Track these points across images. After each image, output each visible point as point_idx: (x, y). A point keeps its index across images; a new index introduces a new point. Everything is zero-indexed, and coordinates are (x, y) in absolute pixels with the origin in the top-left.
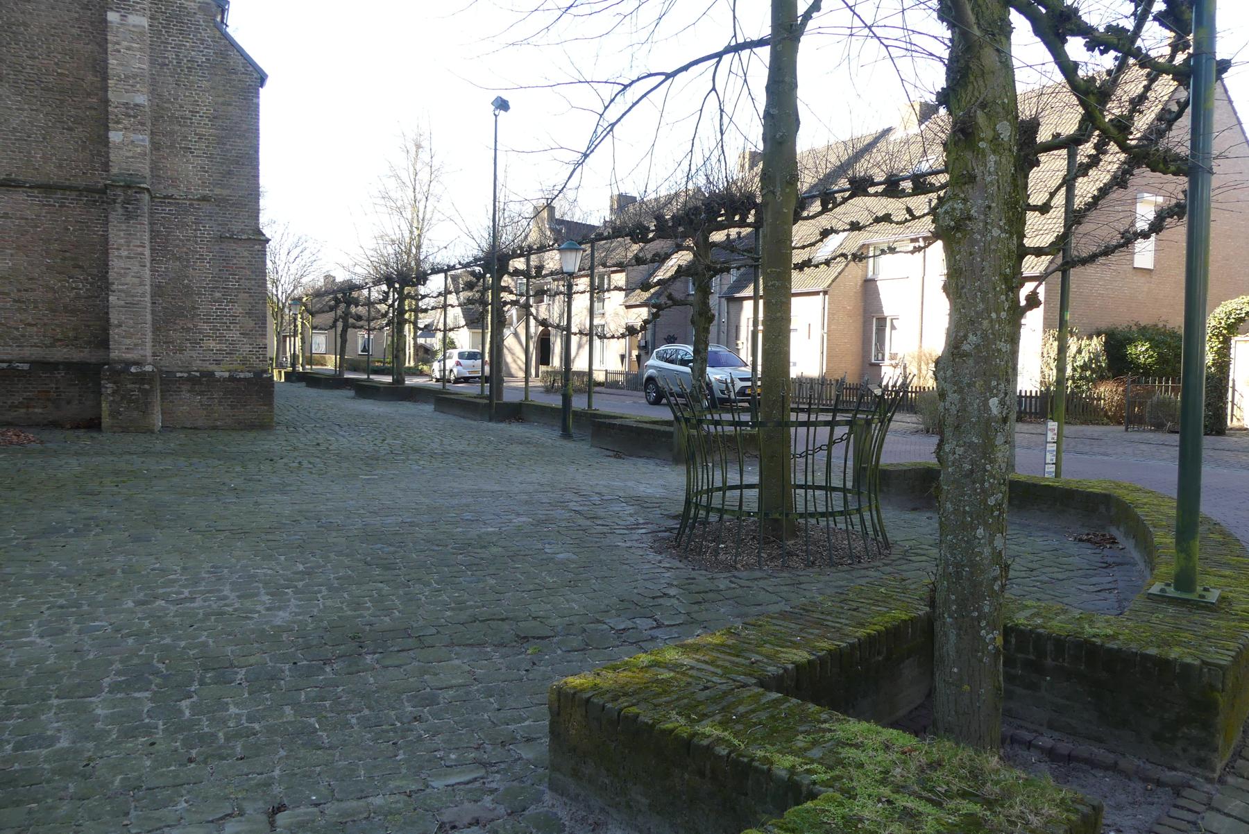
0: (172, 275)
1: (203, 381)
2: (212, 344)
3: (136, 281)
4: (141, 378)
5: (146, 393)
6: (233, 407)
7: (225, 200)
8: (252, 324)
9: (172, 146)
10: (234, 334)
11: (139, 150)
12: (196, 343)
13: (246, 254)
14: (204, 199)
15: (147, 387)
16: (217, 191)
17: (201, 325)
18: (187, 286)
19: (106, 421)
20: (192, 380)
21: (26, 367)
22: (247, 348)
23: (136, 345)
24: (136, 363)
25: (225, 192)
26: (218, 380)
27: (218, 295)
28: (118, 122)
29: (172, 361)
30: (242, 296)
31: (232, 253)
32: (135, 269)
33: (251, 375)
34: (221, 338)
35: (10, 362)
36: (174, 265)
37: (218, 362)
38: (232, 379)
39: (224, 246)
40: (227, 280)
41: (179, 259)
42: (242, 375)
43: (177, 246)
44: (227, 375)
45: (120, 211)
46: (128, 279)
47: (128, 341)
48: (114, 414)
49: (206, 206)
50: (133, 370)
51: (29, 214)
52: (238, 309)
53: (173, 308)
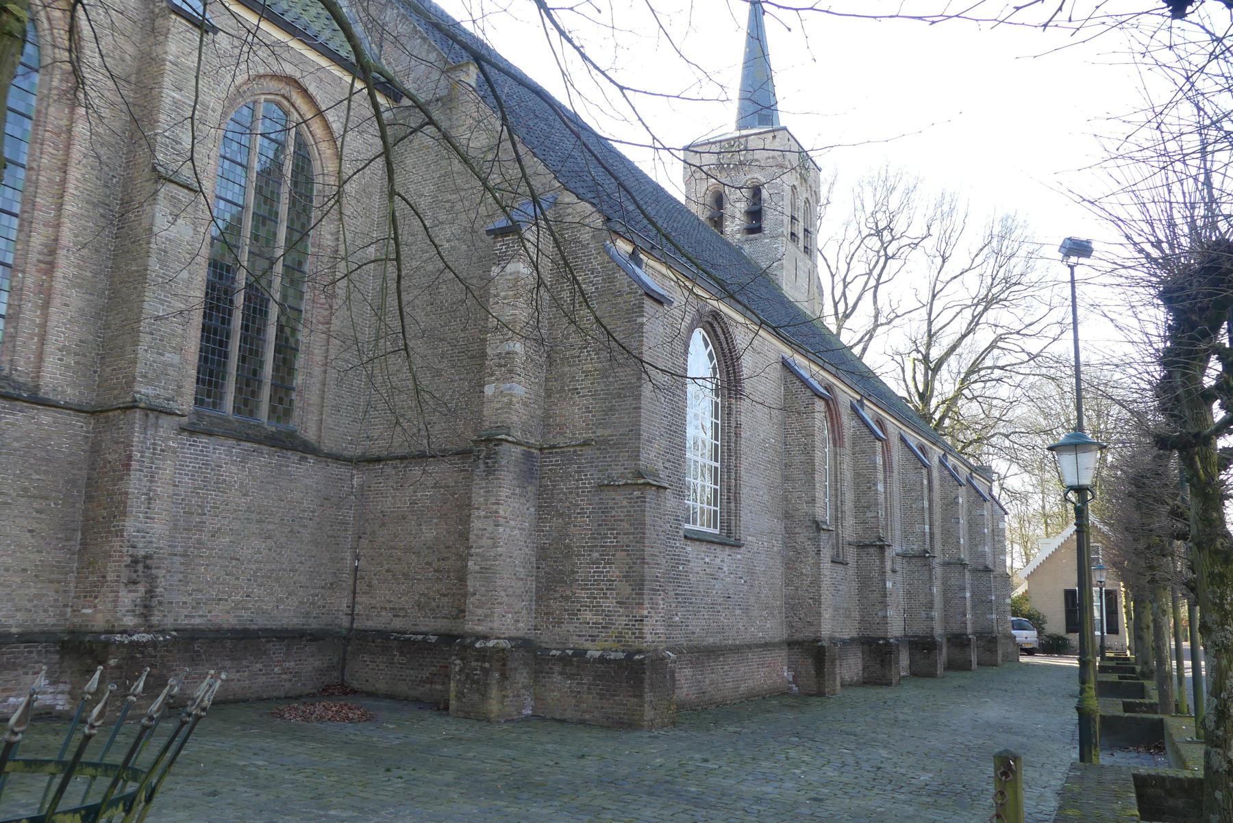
0: (555, 534)
1: (574, 661)
2: (588, 616)
3: (490, 542)
4: (483, 655)
5: (486, 672)
6: (602, 696)
7: (606, 442)
8: (629, 590)
9: (562, 390)
10: (609, 604)
11: (506, 400)
12: (574, 614)
13: (625, 503)
14: (586, 443)
15: (487, 665)
16: (599, 432)
18: (568, 547)
19: (453, 703)
20: (564, 660)
21: (433, 639)
22: (623, 621)
23: (486, 616)
24: (486, 638)
25: (607, 432)
26: (588, 662)
27: (596, 555)
28: (492, 375)
29: (548, 637)
30: (621, 555)
31: (611, 504)
32: (490, 529)
33: (621, 655)
34: (597, 609)
35: (426, 634)
36: (557, 522)
37: (593, 638)
38: (602, 660)
39: (603, 496)
40: (605, 536)
41: (561, 515)
42: (613, 656)
43: (561, 500)
44: (597, 654)
45: (482, 467)
46: (485, 542)
47: (480, 611)
48: (460, 695)
49: (588, 451)
50: (477, 645)
51: (451, 482)
52: (615, 572)
53: (552, 575)
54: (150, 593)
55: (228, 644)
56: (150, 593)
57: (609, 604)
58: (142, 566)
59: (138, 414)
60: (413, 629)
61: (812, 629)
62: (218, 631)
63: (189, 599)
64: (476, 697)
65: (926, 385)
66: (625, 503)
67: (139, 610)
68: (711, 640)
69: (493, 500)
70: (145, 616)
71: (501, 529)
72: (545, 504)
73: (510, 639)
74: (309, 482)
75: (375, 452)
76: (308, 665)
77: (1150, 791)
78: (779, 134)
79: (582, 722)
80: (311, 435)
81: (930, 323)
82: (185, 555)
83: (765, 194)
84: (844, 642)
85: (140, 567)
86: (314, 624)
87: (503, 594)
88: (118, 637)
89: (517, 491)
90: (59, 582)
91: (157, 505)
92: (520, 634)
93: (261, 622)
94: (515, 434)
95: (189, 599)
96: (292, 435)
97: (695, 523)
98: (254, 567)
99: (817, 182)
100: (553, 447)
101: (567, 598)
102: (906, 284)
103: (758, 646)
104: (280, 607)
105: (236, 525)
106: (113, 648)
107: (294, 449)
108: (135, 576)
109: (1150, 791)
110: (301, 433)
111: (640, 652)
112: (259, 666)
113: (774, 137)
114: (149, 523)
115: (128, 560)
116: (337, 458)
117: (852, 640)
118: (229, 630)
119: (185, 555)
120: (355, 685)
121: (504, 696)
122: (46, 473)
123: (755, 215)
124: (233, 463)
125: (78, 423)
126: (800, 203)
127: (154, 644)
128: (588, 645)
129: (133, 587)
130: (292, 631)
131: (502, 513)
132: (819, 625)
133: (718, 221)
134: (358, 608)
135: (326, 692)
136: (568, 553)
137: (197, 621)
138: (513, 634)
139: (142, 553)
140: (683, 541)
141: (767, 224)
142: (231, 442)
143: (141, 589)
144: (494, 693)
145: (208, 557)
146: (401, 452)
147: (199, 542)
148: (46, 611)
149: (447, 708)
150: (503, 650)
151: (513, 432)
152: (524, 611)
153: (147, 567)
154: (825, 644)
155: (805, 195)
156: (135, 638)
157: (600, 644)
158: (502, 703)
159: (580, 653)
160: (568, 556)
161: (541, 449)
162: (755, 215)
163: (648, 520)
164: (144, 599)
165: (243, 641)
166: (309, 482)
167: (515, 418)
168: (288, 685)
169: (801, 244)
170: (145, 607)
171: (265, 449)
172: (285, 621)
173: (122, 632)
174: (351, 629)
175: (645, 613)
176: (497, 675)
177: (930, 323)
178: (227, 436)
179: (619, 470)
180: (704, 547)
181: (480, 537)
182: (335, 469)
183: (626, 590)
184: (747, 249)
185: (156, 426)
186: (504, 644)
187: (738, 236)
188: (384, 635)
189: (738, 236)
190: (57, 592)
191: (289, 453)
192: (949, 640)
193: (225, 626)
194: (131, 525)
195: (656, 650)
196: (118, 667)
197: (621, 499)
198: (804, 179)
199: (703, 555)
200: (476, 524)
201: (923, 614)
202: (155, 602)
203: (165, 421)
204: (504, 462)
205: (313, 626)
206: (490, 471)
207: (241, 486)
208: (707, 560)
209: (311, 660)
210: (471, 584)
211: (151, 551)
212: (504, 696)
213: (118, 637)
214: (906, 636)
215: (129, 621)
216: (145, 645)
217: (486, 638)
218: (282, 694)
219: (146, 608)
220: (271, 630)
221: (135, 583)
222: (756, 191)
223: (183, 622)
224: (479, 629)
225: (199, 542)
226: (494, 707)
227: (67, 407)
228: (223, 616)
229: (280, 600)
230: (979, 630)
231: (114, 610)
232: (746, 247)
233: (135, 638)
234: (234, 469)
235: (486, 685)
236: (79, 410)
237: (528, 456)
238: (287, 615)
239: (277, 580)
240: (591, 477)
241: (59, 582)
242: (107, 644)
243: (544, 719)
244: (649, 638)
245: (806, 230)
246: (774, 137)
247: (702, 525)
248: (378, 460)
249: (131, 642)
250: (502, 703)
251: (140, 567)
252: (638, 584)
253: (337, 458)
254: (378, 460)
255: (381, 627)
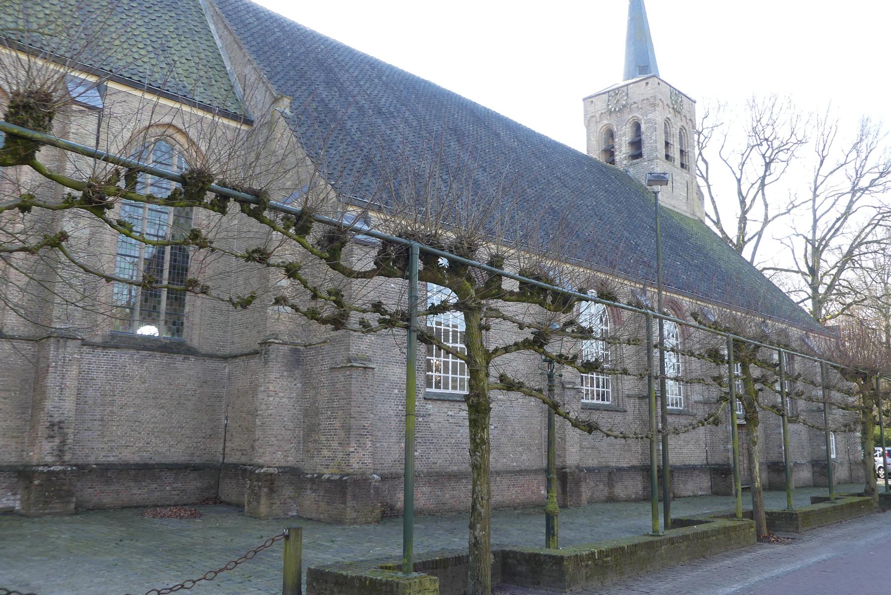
1: (317, 481)
4: (259, 477)
5: (260, 488)
6: (328, 504)
12: (319, 451)
14: (325, 342)
17: (323, 438)
18: (317, 408)
20: (312, 480)
33: (338, 477)
34: (329, 448)
36: (313, 392)
38: (329, 480)
46: (264, 407)
47: (261, 450)
48: (249, 502)
49: (327, 347)
52: (337, 424)
53: (309, 427)
54: (63, 442)
55: (132, 472)
56: (63, 442)
57: (335, 444)
58: (56, 428)
59: (52, 340)
60: (250, 462)
61: (561, 460)
62: (126, 465)
63: (106, 446)
64: (255, 503)
65: (814, 262)
66: (342, 379)
67: (55, 453)
68: (455, 468)
69: (267, 380)
70: (60, 456)
71: (271, 399)
72: (308, 382)
73: (278, 468)
74: (191, 372)
75: (235, 352)
76: (193, 485)
77: (510, 561)
78: (650, 81)
79: (319, 521)
80: (195, 343)
81: (815, 211)
82: (102, 420)
83: (643, 127)
84: (620, 469)
85: (56, 428)
86: (197, 460)
87: (273, 439)
88: (41, 468)
89: (285, 374)
90: (18, 437)
91: (67, 392)
92: (289, 464)
93: (157, 459)
94: (282, 338)
95: (106, 446)
96: (181, 344)
97: (446, 387)
98: (152, 426)
99: (692, 112)
100: (310, 345)
101: (316, 441)
102: (792, 181)
103: (508, 472)
104: (174, 451)
105: (137, 401)
106: (37, 474)
107: (178, 353)
108: (52, 433)
109: (510, 561)
110: (188, 343)
111: (348, 475)
112: (155, 486)
113: (647, 83)
114: (61, 403)
115: (48, 424)
116: (211, 356)
117: (633, 468)
118: (134, 465)
119: (102, 420)
120: (223, 498)
121: (273, 503)
122: (8, 376)
123: (637, 144)
124: (134, 364)
125: (27, 347)
126: (675, 130)
127: (64, 472)
128: (325, 471)
129: (51, 440)
130: (182, 464)
131: (271, 388)
132: (565, 456)
133: (610, 152)
134: (227, 450)
135: (205, 502)
136: (317, 413)
137: (112, 459)
138: (283, 464)
139: (57, 420)
140: (423, 401)
141: (645, 151)
142: (132, 351)
143: (57, 441)
144: (263, 500)
145: (118, 421)
146: (246, 351)
147: (112, 412)
148: (10, 454)
149: (243, 511)
150: (271, 474)
151: (280, 336)
152: (293, 450)
153: (60, 428)
154: (568, 470)
155: (679, 124)
156: (52, 469)
157: (330, 470)
158: (271, 507)
159: (320, 475)
160: (317, 415)
161: (305, 346)
162: (637, 144)
163: (354, 389)
164: (59, 446)
165: (144, 471)
166: (191, 372)
167: (282, 328)
168: (176, 498)
169: (678, 162)
170: (60, 451)
171: (158, 354)
172: (175, 459)
173: (45, 465)
174: (223, 463)
175: (352, 449)
176: (266, 490)
177: (815, 211)
178: (128, 348)
179: (340, 359)
180: (447, 404)
181: (261, 404)
182: (211, 364)
183: (342, 434)
184: (632, 172)
185: (65, 347)
186: (271, 470)
187: (625, 162)
188: (235, 466)
189: (625, 162)
190: (17, 443)
191: (176, 356)
192: (769, 467)
193: (131, 462)
194: (48, 405)
195: (363, 474)
196: (39, 485)
197: (340, 376)
198: (677, 112)
199: (446, 410)
200: (260, 396)
201: (722, 447)
202: (66, 448)
203: (70, 343)
204: (272, 357)
205: (197, 461)
206: (266, 362)
207: (141, 377)
208: (450, 413)
209: (194, 483)
210: (258, 433)
211: (63, 419)
212: (273, 503)
213: (41, 468)
214: (708, 464)
215: (49, 459)
216: (58, 472)
217: (262, 467)
218: (172, 503)
219: (60, 452)
220: (165, 464)
221: (53, 437)
222: (637, 126)
223: (102, 459)
224: (261, 461)
225: (112, 412)
226: (263, 509)
227: (20, 338)
228: (130, 455)
229: (171, 446)
230: (815, 458)
231: (43, 453)
232: (631, 170)
233: (52, 469)
234: (135, 368)
235: (260, 496)
236: (28, 340)
237: (295, 351)
238: (177, 453)
239: (169, 433)
240: (327, 363)
241: (18, 437)
242: (34, 472)
243: (301, 518)
244: (356, 466)
245: (682, 151)
246: (647, 83)
247: (454, 388)
248: (236, 357)
249: (49, 471)
250: (271, 507)
251: (56, 428)
252: (348, 429)
253: (211, 356)
254: (236, 357)
255: (235, 461)
